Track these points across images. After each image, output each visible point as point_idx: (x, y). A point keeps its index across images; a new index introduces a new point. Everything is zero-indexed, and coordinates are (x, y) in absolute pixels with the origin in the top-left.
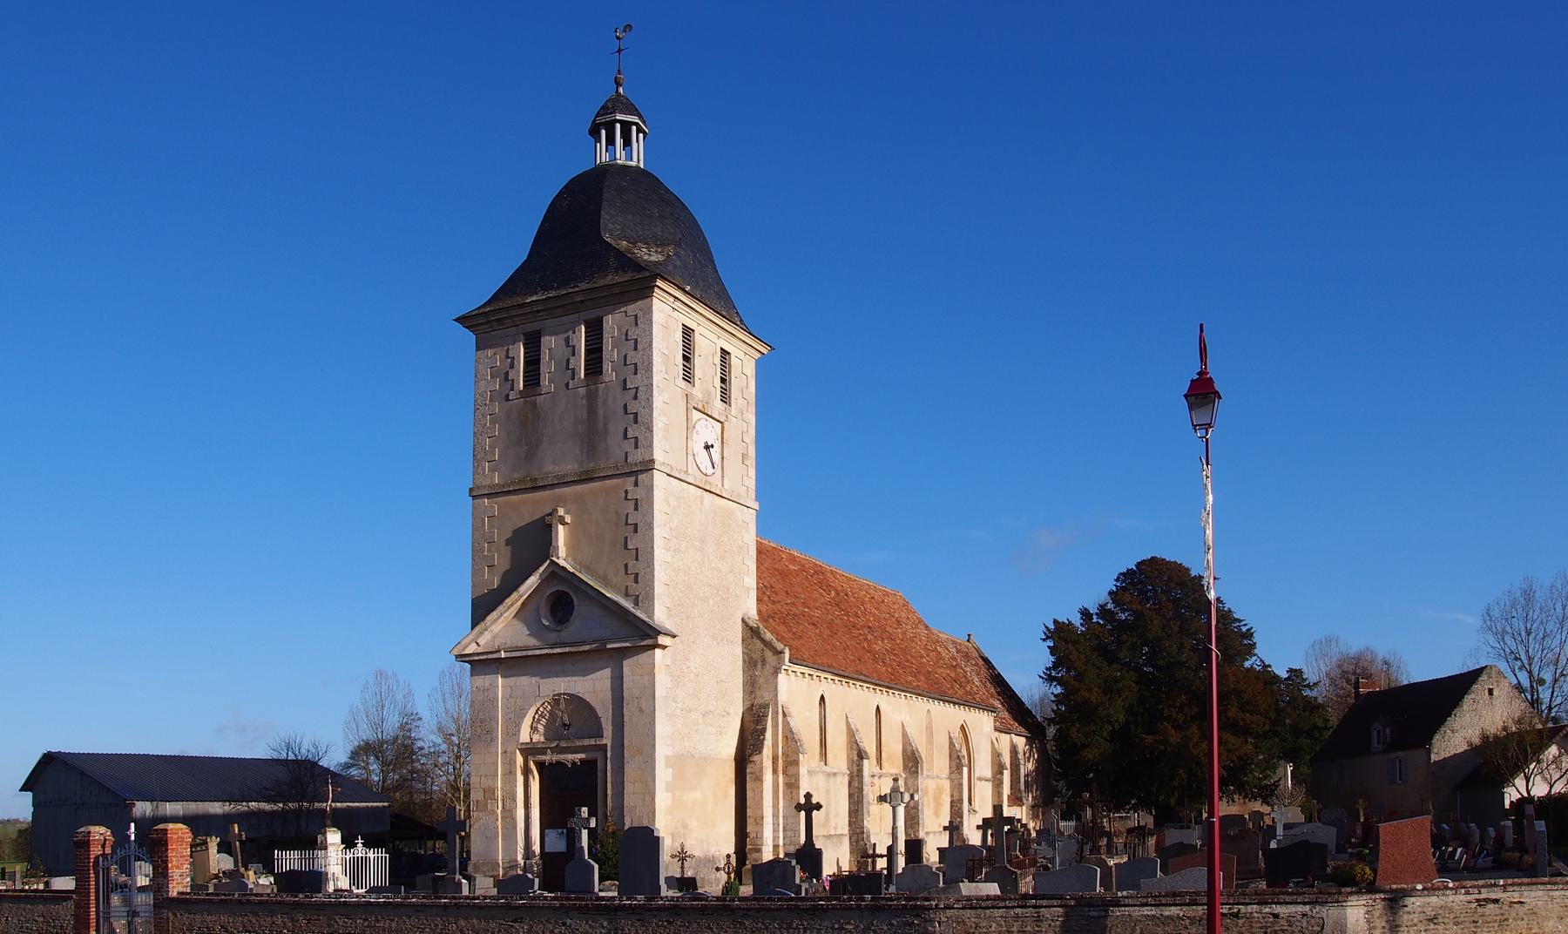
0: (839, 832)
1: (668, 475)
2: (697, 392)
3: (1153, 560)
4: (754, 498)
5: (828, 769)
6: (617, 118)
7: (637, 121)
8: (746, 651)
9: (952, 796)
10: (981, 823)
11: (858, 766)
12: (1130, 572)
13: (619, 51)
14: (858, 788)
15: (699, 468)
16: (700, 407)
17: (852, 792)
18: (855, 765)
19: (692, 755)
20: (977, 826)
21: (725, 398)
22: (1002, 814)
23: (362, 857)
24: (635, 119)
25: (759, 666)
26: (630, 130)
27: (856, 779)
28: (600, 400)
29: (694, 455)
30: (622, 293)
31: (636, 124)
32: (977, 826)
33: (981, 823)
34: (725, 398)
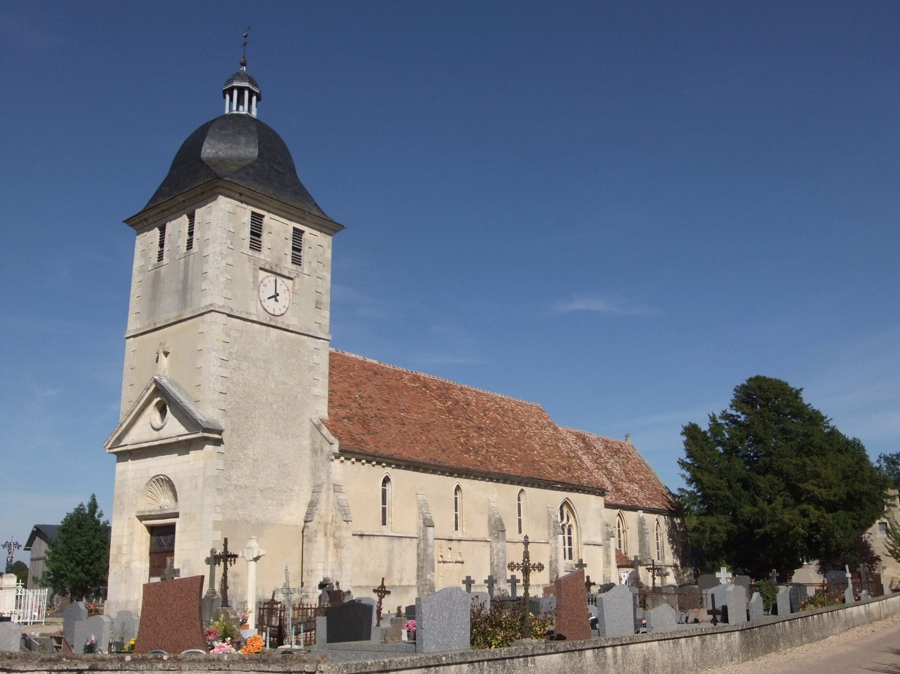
0: (405, 583)
1: (229, 315)
2: (265, 256)
3: (758, 378)
4: (328, 332)
5: (386, 530)
6: (234, 85)
7: (247, 86)
8: (311, 443)
9: (551, 557)
10: (487, 579)
11: (423, 531)
12: (743, 386)
13: (245, 44)
14: (423, 549)
15: (266, 310)
16: (267, 267)
17: (419, 552)
18: (421, 531)
19: (246, 521)
20: (470, 577)
21: (297, 261)
22: (173, 567)
23: (21, 596)
24: (246, 84)
25: (319, 454)
26: (243, 94)
27: (422, 541)
28: (190, 266)
29: (261, 301)
30: (202, 193)
31: (248, 88)
32: (470, 577)
33: (487, 579)
34: (297, 261)
